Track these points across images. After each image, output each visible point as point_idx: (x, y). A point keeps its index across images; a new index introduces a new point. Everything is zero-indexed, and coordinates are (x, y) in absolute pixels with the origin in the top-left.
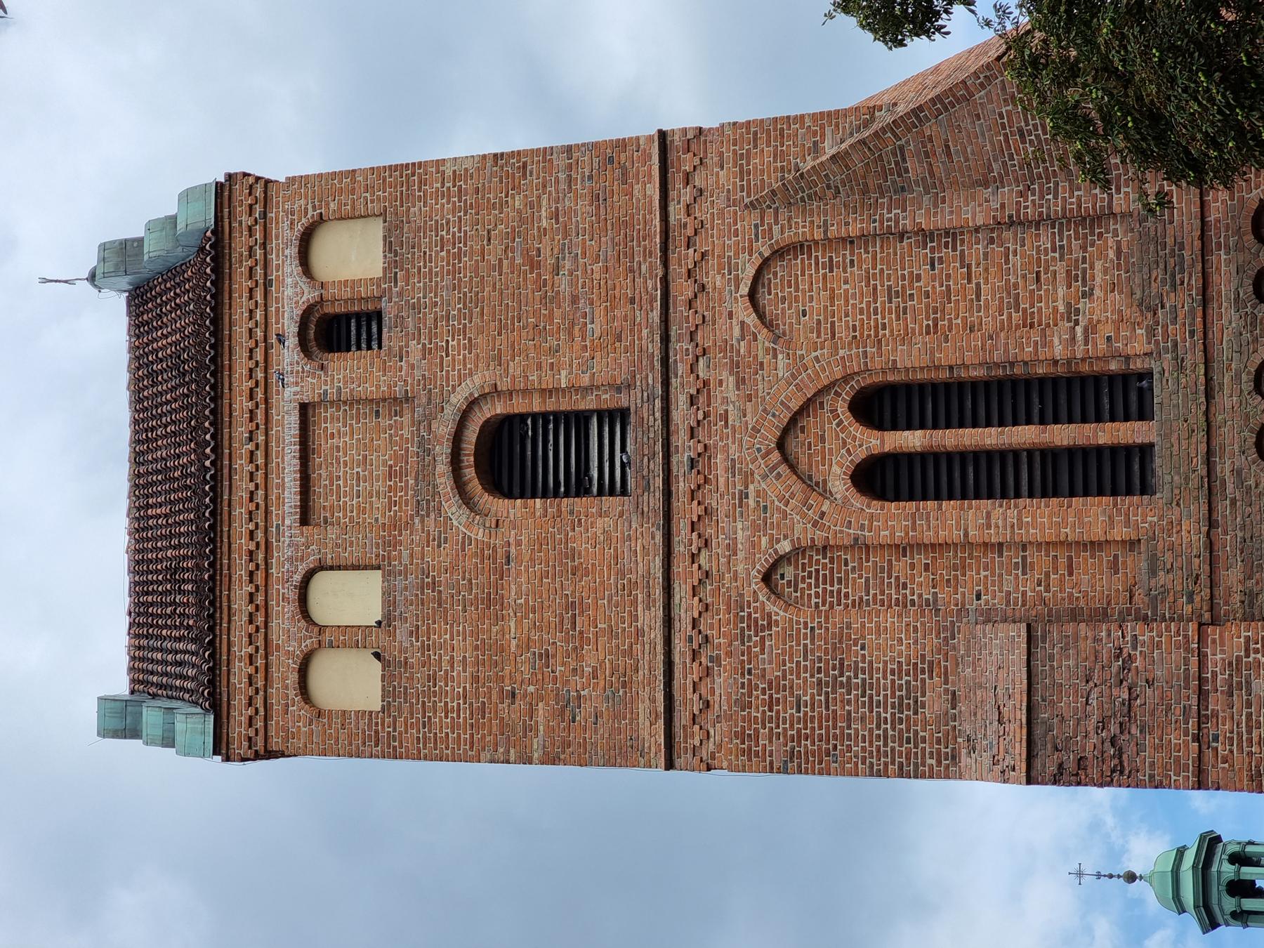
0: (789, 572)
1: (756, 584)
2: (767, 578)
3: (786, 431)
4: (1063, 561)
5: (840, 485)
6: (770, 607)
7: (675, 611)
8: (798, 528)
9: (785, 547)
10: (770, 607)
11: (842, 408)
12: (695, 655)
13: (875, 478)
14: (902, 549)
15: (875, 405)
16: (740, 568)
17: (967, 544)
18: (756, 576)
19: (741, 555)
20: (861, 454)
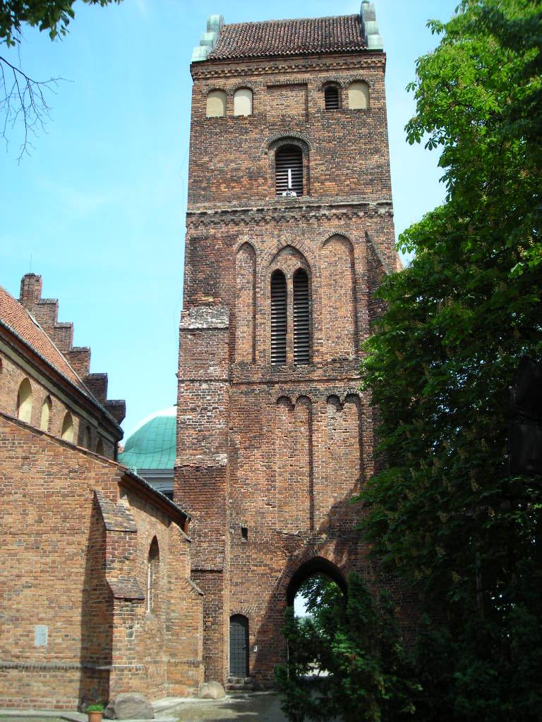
3: (294, 248)
5: (274, 267)
11: (299, 265)
13: (278, 277)
15: (302, 277)
20: (285, 272)
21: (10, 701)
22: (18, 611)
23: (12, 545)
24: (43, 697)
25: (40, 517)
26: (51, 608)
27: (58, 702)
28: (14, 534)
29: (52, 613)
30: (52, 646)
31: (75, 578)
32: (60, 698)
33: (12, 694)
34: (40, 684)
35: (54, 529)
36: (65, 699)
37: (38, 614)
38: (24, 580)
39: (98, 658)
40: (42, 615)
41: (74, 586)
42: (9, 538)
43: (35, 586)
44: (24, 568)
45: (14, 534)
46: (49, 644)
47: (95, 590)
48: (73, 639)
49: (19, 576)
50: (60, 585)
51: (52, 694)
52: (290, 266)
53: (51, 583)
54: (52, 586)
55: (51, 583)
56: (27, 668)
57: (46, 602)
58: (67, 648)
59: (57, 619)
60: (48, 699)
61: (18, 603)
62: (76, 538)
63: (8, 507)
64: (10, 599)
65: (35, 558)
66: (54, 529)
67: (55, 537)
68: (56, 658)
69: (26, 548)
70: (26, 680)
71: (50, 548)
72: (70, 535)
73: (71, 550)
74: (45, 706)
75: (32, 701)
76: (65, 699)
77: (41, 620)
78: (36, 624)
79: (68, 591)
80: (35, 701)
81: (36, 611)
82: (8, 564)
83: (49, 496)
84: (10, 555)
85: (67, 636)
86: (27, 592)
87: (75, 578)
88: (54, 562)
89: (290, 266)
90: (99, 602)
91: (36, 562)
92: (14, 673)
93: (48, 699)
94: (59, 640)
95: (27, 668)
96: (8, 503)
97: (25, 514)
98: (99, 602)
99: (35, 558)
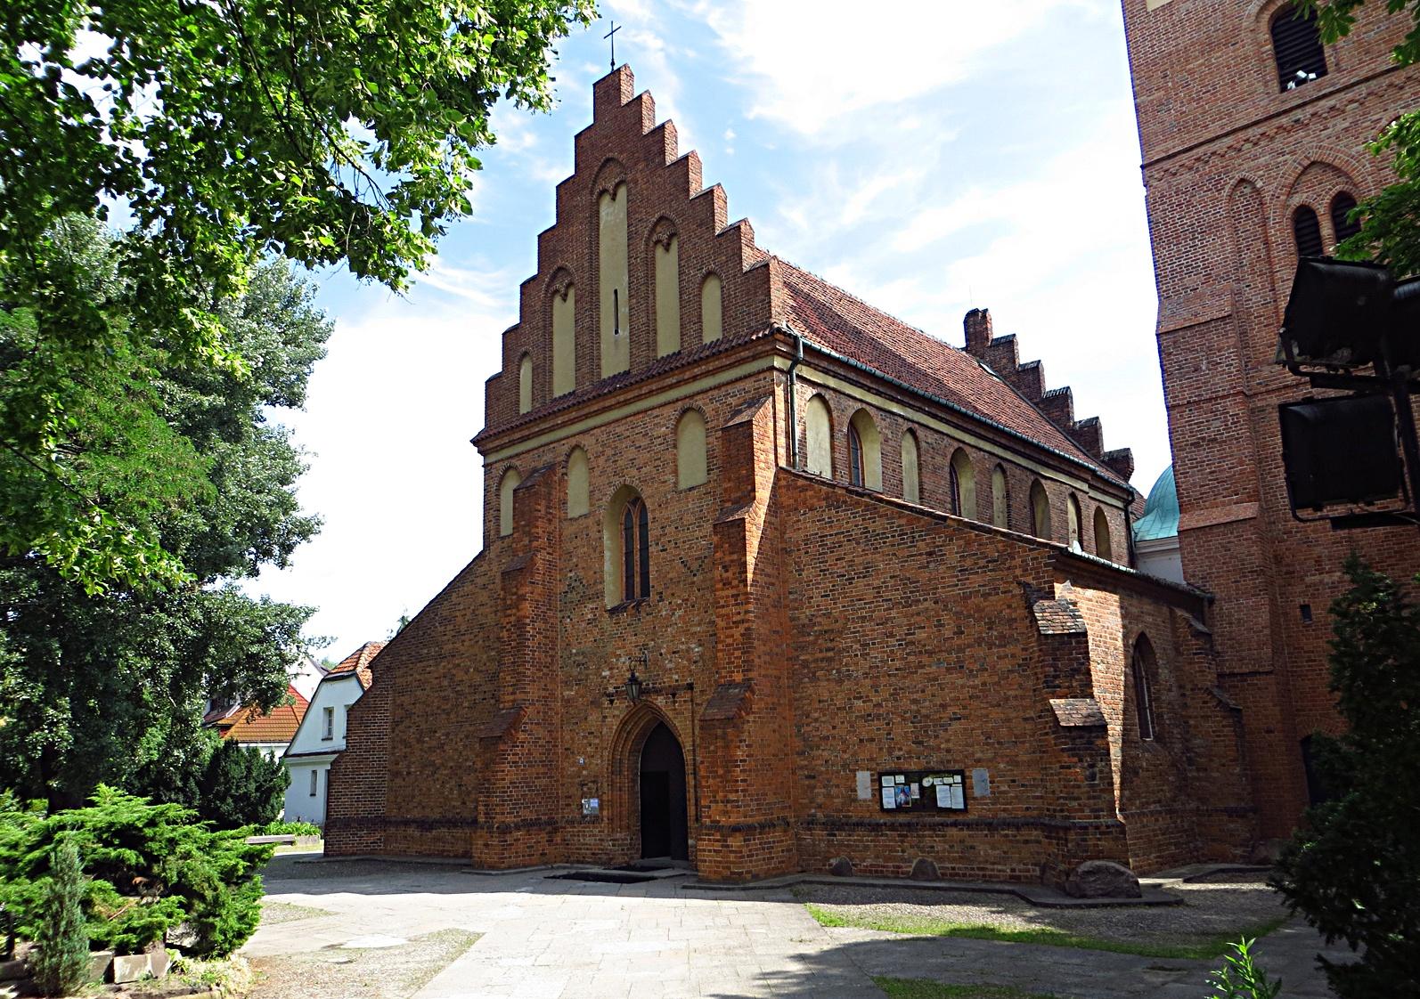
0: (1248, 190)
1: (1238, 176)
2: (1242, 181)
4: (1271, 321)
6: (1227, 188)
7: (1217, 142)
8: (1270, 188)
9: (1259, 184)
10: (1227, 188)
12: (1198, 160)
13: (1304, 219)
14: (1266, 243)
16: (1245, 166)
17: (1272, 273)
18: (1244, 174)
19: (1252, 164)
21: (953, 869)
22: (948, 751)
23: (930, 666)
24: (994, 864)
25: (959, 627)
26: (988, 744)
27: (1013, 870)
28: (930, 653)
29: (990, 755)
30: (996, 796)
31: (1015, 703)
32: (1014, 865)
33: (954, 860)
34: (987, 847)
35: (979, 641)
36: (1022, 866)
37: (973, 754)
38: (950, 710)
39: (1055, 810)
40: (978, 755)
41: (1014, 715)
42: (925, 659)
43: (966, 718)
44: (949, 696)
45: (930, 653)
46: (992, 793)
47: (1040, 717)
48: (1023, 786)
49: (944, 706)
50: (996, 714)
51: (1004, 859)
52: (1319, 197)
53: (984, 712)
54: (987, 716)
55: (984, 712)
56: (968, 825)
57: (982, 738)
58: (1016, 797)
59: (999, 759)
60: (1000, 867)
61: (948, 741)
62: (1009, 650)
63: (917, 619)
64: (937, 737)
65: (960, 682)
66: (979, 641)
67: (981, 652)
68: (1004, 810)
69: (948, 669)
70: (969, 842)
71: (977, 666)
72: (1000, 646)
73: (1005, 665)
74: (998, 877)
75: (979, 869)
76: (1022, 866)
77: (978, 761)
78: (972, 766)
79: (1009, 720)
80: (983, 869)
81: (971, 749)
82: (929, 691)
83: (966, 598)
84: (929, 680)
85: (1014, 781)
86: (956, 726)
87: (1015, 703)
88: (984, 684)
89: (1319, 197)
90: (1047, 734)
91: (963, 686)
92: (953, 832)
93: (1000, 867)
94: (1004, 788)
95: (968, 825)
96: (918, 614)
97: (940, 625)
98: (1047, 734)
99: (960, 682)
